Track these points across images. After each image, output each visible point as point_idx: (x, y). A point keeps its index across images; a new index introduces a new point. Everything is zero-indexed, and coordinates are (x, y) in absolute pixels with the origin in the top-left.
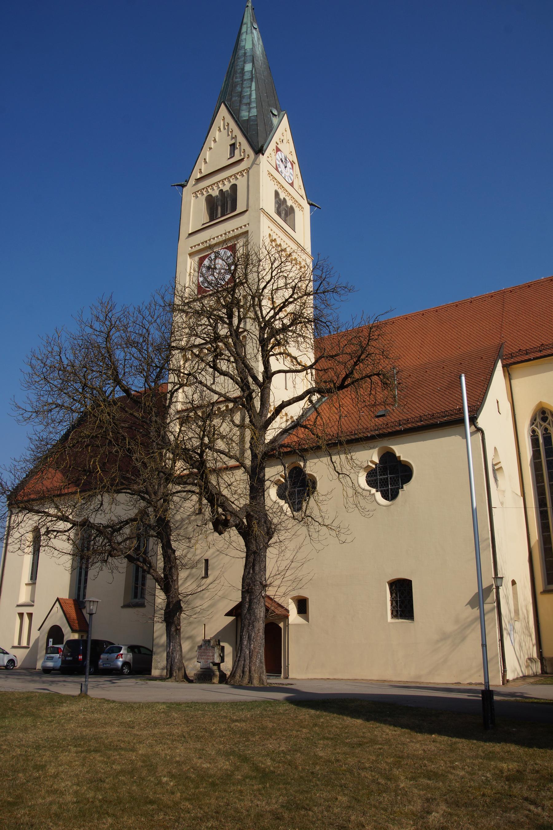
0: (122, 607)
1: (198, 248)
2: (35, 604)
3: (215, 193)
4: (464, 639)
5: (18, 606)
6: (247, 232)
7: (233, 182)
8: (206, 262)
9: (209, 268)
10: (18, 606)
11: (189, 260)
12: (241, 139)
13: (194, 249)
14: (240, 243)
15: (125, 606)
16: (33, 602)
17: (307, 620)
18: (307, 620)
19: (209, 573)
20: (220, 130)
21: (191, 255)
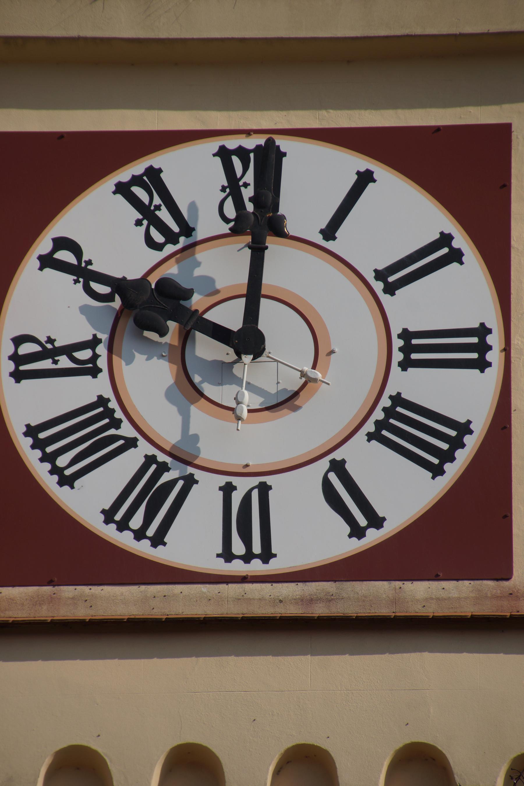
9: (149, 308)
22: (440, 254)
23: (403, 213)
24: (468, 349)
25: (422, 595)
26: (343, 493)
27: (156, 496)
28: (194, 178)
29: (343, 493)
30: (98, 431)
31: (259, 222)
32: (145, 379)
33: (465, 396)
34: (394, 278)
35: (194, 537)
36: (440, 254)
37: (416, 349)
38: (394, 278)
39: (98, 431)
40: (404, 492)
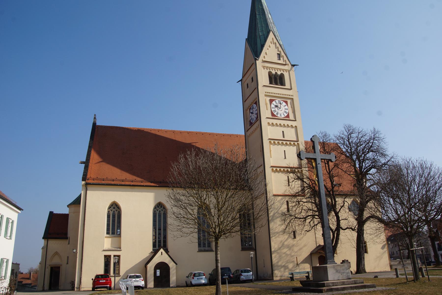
1: (268, 94)
3: (274, 72)
4: (382, 258)
5: (104, 250)
6: (293, 99)
7: (282, 72)
8: (274, 102)
10: (104, 250)
12: (283, 54)
13: (267, 94)
14: (289, 101)
15: (200, 251)
16: (120, 248)
19: (297, 236)
21: (265, 95)
22: (285, 106)
23: (284, 104)
24: (287, 109)
25: (287, 119)
26: (284, 114)
27: (277, 114)
28: (277, 101)
29: (284, 114)
32: (276, 109)
33: (287, 111)
34: (285, 106)
36: (285, 106)
37: (285, 109)
38: (285, 106)
39: (275, 111)
40: (286, 115)
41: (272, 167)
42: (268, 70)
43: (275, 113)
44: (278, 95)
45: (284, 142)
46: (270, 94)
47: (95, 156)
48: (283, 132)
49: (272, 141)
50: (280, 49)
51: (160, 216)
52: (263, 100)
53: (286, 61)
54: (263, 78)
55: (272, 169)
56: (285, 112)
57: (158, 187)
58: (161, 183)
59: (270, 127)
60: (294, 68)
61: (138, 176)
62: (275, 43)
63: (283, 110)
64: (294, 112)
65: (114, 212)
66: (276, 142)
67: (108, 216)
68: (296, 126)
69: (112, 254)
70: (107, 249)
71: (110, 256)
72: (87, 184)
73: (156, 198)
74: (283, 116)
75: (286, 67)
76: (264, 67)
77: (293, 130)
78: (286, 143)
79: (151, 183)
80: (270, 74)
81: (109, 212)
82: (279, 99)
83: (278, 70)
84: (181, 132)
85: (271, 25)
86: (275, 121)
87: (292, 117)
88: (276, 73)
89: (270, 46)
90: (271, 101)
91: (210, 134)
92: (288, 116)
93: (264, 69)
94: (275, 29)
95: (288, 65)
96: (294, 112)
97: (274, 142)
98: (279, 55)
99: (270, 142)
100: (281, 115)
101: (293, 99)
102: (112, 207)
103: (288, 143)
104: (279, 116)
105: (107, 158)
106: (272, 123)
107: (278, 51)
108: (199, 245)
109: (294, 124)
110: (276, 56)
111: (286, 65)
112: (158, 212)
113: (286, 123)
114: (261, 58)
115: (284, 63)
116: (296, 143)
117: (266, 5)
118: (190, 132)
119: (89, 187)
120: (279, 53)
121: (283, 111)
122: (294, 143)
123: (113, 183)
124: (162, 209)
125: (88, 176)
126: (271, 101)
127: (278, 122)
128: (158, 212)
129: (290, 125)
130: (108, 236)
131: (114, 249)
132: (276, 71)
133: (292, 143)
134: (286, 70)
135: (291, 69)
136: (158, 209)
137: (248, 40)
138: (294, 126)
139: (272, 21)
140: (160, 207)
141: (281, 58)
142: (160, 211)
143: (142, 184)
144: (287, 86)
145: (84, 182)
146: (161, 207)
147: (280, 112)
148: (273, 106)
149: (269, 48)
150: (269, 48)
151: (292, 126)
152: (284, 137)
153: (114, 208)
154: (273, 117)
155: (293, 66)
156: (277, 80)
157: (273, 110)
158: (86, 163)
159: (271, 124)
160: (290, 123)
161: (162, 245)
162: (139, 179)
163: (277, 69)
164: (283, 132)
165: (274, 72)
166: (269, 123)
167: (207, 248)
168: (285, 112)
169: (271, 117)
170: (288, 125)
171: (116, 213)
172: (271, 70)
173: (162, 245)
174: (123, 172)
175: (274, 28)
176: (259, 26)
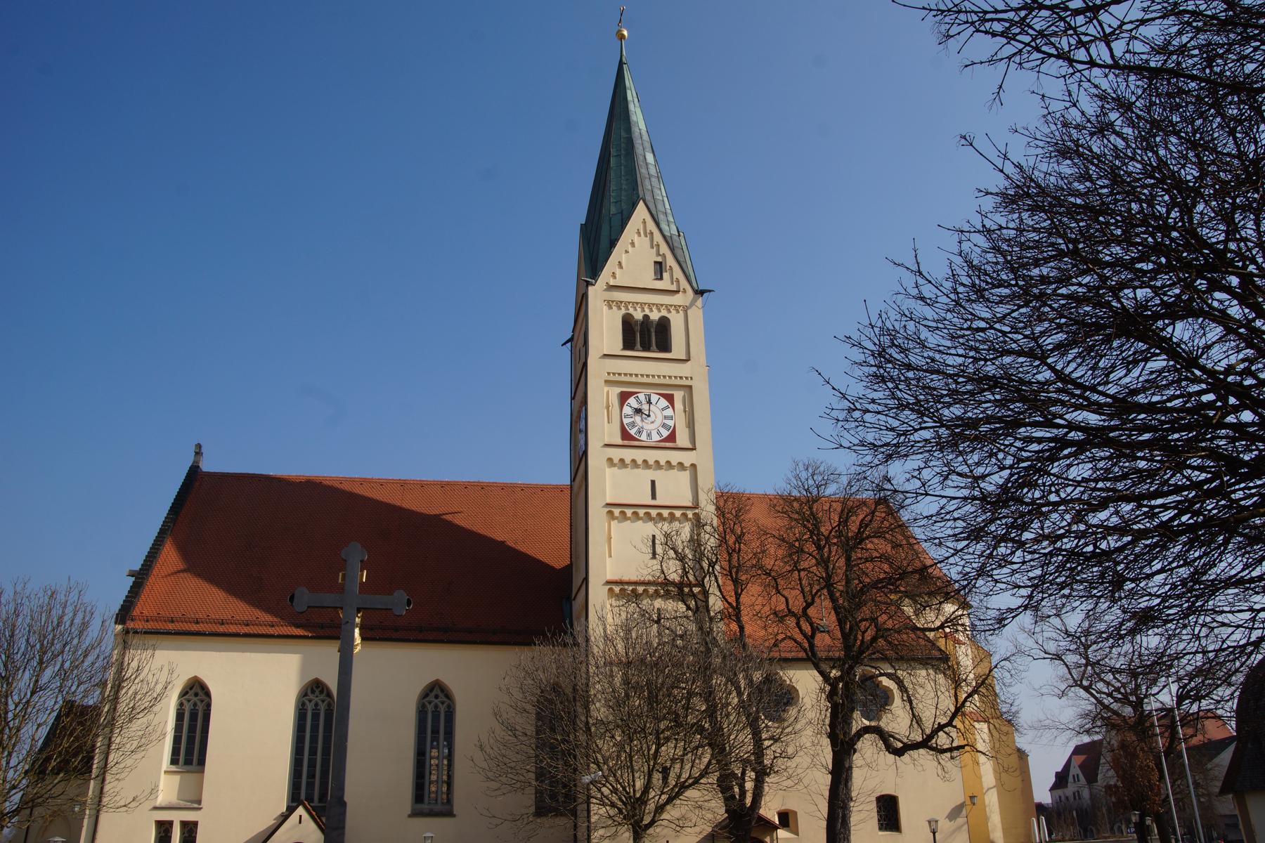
0: (410, 816)
1: (617, 378)
2: (204, 804)
3: (638, 315)
5: (156, 808)
6: (690, 387)
7: (664, 313)
8: (632, 401)
10: (156, 808)
11: (606, 389)
12: (670, 261)
13: (612, 378)
14: (679, 396)
15: (415, 814)
16: (199, 802)
17: (797, 834)
18: (797, 834)
20: (639, 233)
21: (607, 382)
23: (664, 403)
25: (668, 445)
27: (639, 432)
28: (642, 397)
29: (659, 433)
30: (633, 424)
31: (649, 402)
32: (638, 419)
33: (671, 423)
34: (663, 409)
35: (644, 437)
37: (666, 417)
38: (663, 409)
39: (633, 424)
40: (665, 433)
41: (608, 583)
42: (623, 311)
43: (633, 432)
44: (645, 380)
45: (654, 512)
46: (623, 378)
47: (170, 556)
48: (653, 483)
49: (617, 511)
50: (664, 249)
51: (316, 716)
52: (600, 395)
53: (678, 281)
54: (605, 332)
55: (611, 590)
56: (664, 426)
57: (312, 638)
58: (322, 627)
59: (609, 472)
60: (700, 302)
61: (267, 610)
62: (652, 233)
63: (659, 420)
64: (691, 424)
65: (195, 705)
66: (629, 512)
67: (180, 716)
68: (693, 466)
69: (177, 817)
70: (163, 805)
71: (171, 823)
72: (127, 632)
73: (304, 668)
74: (656, 437)
75: (678, 300)
76: (609, 303)
77: (686, 476)
78: (659, 515)
79: (297, 626)
80: (628, 323)
81: (181, 704)
82: (648, 391)
83: (649, 308)
84: (422, 485)
85: (647, 183)
86: (628, 455)
87: (682, 439)
88: (646, 317)
89: (633, 244)
90: (624, 397)
91: (503, 487)
92: (672, 437)
93: (610, 307)
94: (661, 194)
95: (685, 291)
96: (691, 424)
97: (623, 513)
98: (660, 268)
99: (610, 513)
100: (649, 435)
101: (690, 387)
102: (191, 692)
103: (665, 513)
104: (644, 437)
105: (199, 562)
106: (622, 460)
107: (658, 254)
108: (419, 796)
109: (687, 458)
110: (651, 269)
111: (678, 292)
112: (310, 707)
113: (663, 456)
114: (605, 277)
115: (674, 288)
116: (690, 514)
117: (642, 125)
118: (448, 483)
119: (136, 640)
120: (659, 259)
121: (658, 418)
122: (684, 515)
123: (194, 628)
124: (322, 697)
125: (136, 612)
126: (624, 397)
127: (640, 455)
128: (310, 707)
129: (674, 463)
130: (173, 768)
131: (183, 804)
132: (647, 312)
133: (678, 513)
134: (677, 308)
135: (693, 303)
136: (311, 696)
137: (584, 228)
138: (687, 464)
139: (653, 171)
140: (317, 692)
141: (666, 275)
142: (316, 705)
143: (271, 631)
144: (678, 350)
145: (119, 627)
146: (321, 692)
147: (648, 426)
148: (627, 410)
149: (630, 249)
150: (630, 249)
151: (681, 464)
152: (654, 496)
153: (196, 695)
154: (626, 443)
155: (699, 293)
156: (646, 336)
157: (626, 421)
158: (140, 578)
159: (616, 461)
160: (675, 457)
161: (303, 796)
162: (268, 618)
163: (650, 305)
164: (653, 483)
165: (638, 315)
166: (610, 460)
167: (438, 808)
168: (664, 426)
169: (619, 442)
170: (668, 462)
171: (200, 707)
172: (631, 311)
173: (303, 796)
174: (232, 599)
175: (657, 192)
176: (613, 187)
